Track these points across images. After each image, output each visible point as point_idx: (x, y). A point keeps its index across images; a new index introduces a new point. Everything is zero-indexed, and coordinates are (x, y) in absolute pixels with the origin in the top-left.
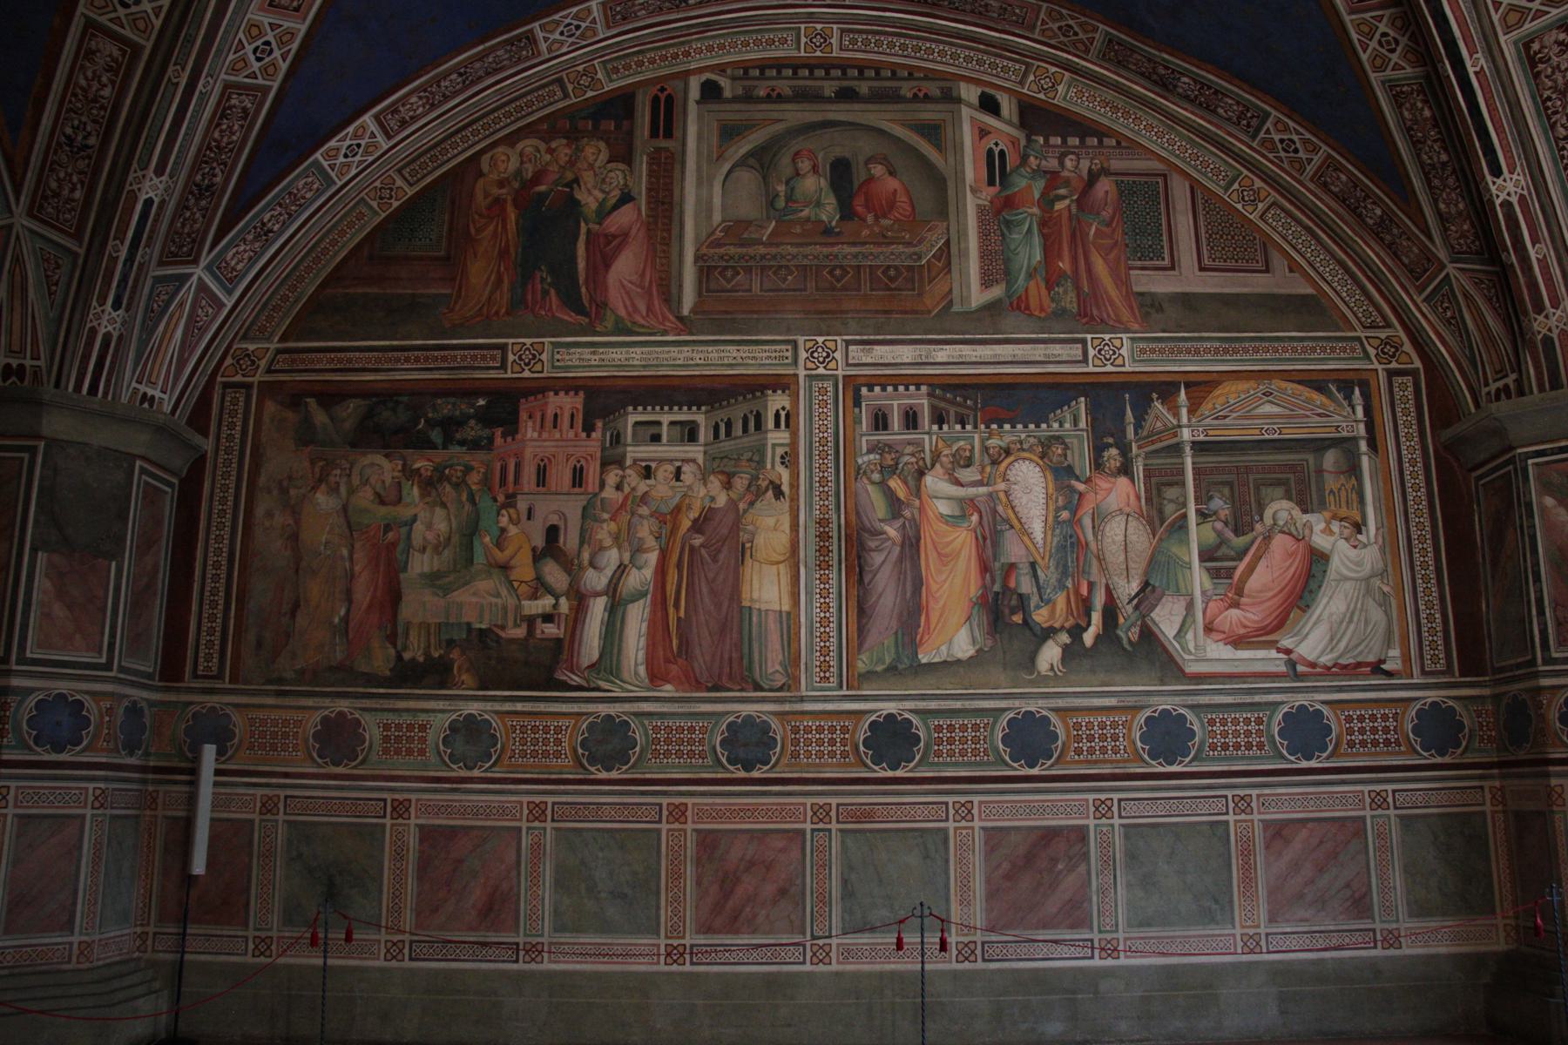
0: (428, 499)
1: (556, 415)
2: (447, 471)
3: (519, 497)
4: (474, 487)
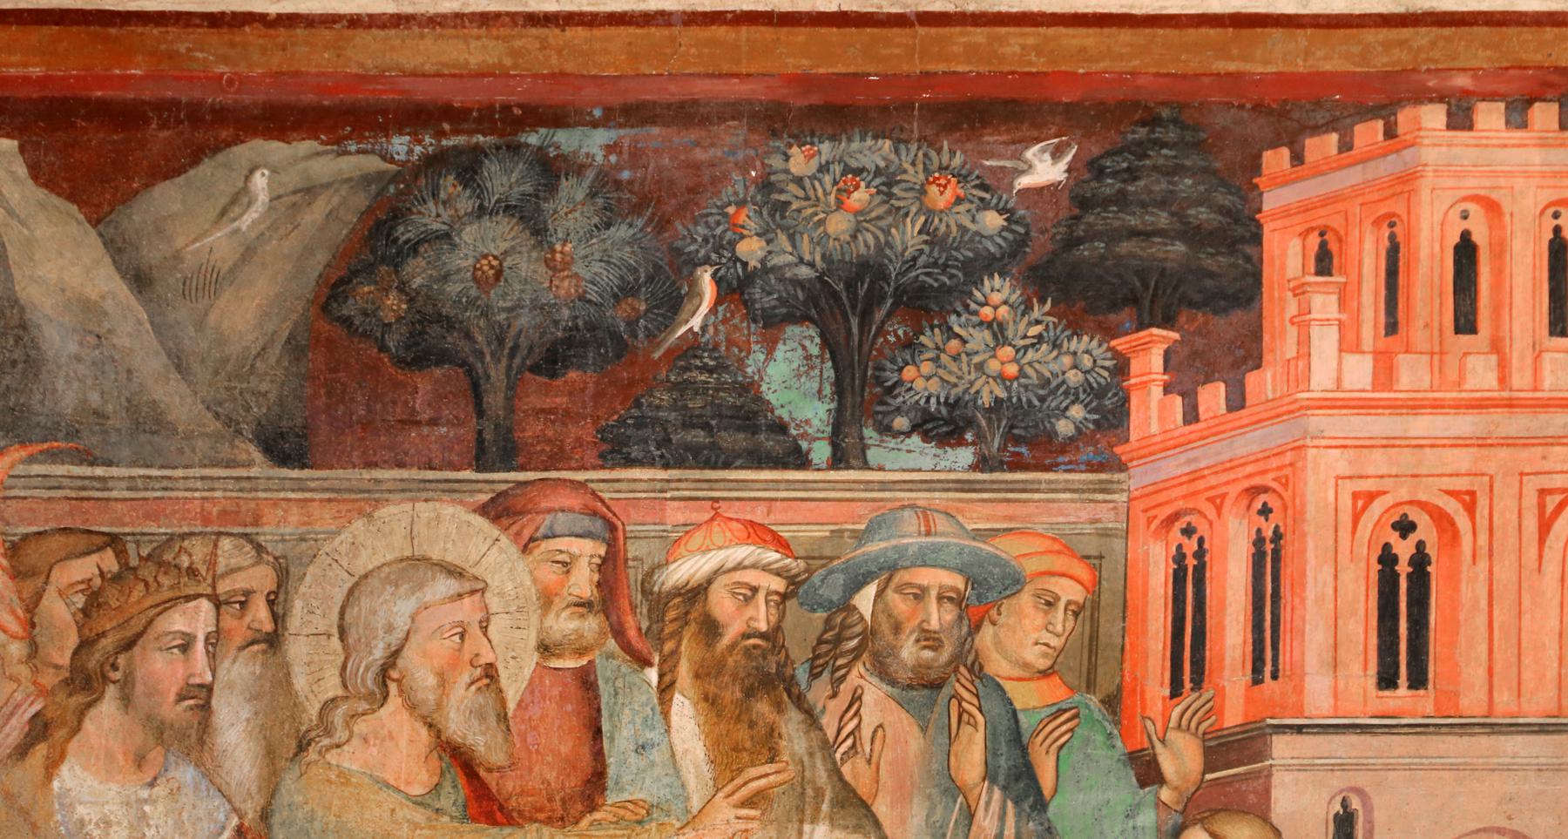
0: (761, 776)
1: (1466, 252)
2: (865, 601)
3: (1282, 748)
4: (1028, 697)
